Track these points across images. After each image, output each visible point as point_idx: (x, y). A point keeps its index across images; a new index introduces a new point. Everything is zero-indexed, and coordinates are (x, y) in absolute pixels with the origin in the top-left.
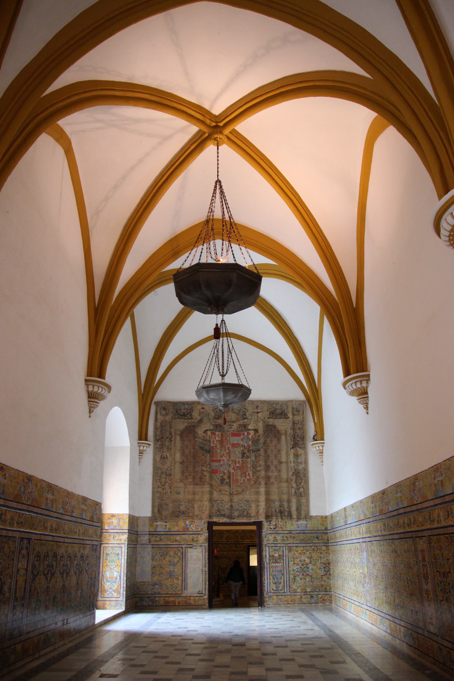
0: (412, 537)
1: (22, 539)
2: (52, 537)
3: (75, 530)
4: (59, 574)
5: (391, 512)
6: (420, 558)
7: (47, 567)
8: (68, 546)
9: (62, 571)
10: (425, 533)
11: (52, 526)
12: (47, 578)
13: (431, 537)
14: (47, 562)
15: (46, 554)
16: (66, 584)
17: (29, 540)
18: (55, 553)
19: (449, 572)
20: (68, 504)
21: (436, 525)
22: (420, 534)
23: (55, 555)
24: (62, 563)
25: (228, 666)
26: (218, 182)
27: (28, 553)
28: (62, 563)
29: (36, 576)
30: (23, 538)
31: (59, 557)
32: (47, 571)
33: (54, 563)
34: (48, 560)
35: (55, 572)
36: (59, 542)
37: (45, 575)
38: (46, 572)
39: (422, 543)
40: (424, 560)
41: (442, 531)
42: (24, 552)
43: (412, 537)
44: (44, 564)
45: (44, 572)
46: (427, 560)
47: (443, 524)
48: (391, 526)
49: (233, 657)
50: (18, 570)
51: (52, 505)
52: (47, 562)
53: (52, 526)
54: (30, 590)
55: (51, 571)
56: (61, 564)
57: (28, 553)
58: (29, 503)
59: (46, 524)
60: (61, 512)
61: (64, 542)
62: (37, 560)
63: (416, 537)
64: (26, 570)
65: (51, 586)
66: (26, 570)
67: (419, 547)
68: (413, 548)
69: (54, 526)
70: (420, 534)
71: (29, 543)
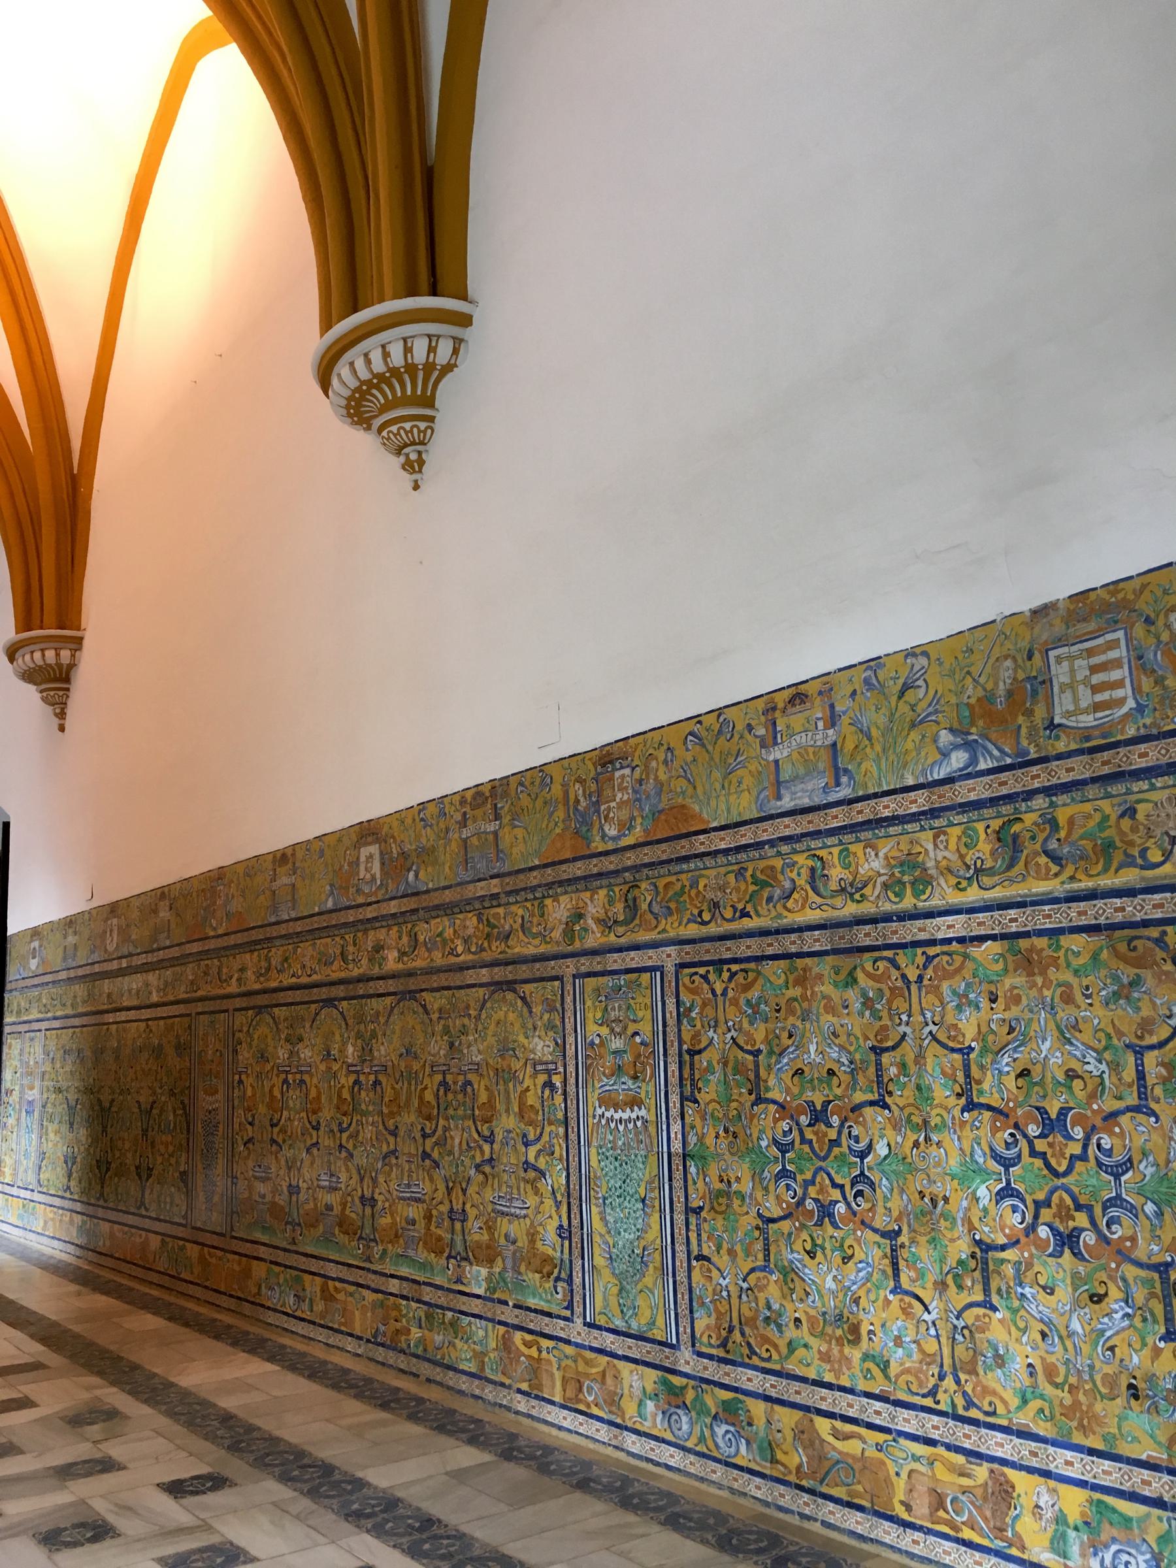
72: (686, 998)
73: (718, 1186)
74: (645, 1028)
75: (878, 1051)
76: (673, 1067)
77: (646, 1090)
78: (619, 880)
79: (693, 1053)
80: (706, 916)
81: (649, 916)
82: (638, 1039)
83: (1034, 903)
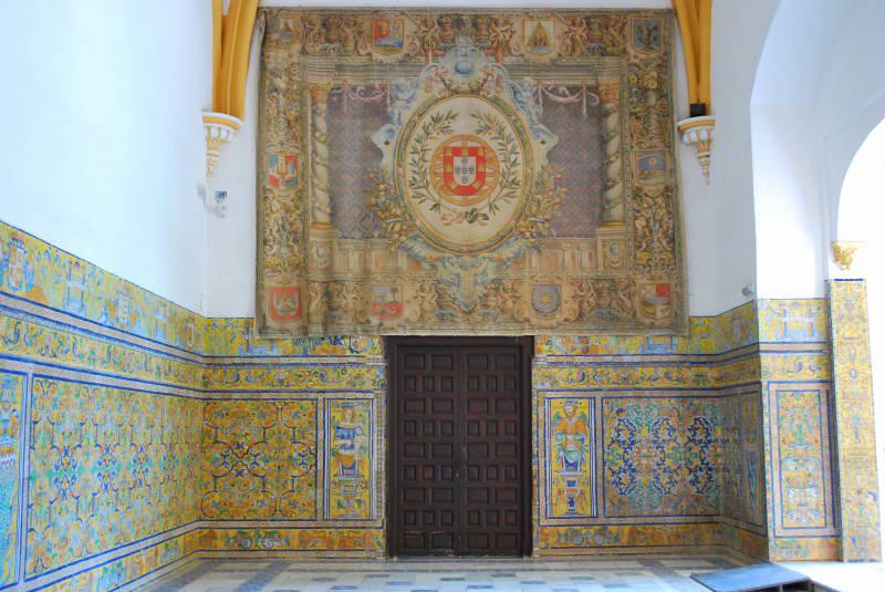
72: (35, 393)
73: (39, 491)
74: (18, 407)
75: (82, 424)
76: (28, 430)
77: (16, 443)
78: (16, 316)
79: (36, 423)
80: (44, 351)
81: (24, 343)
82: (15, 414)
83: (68, 369)
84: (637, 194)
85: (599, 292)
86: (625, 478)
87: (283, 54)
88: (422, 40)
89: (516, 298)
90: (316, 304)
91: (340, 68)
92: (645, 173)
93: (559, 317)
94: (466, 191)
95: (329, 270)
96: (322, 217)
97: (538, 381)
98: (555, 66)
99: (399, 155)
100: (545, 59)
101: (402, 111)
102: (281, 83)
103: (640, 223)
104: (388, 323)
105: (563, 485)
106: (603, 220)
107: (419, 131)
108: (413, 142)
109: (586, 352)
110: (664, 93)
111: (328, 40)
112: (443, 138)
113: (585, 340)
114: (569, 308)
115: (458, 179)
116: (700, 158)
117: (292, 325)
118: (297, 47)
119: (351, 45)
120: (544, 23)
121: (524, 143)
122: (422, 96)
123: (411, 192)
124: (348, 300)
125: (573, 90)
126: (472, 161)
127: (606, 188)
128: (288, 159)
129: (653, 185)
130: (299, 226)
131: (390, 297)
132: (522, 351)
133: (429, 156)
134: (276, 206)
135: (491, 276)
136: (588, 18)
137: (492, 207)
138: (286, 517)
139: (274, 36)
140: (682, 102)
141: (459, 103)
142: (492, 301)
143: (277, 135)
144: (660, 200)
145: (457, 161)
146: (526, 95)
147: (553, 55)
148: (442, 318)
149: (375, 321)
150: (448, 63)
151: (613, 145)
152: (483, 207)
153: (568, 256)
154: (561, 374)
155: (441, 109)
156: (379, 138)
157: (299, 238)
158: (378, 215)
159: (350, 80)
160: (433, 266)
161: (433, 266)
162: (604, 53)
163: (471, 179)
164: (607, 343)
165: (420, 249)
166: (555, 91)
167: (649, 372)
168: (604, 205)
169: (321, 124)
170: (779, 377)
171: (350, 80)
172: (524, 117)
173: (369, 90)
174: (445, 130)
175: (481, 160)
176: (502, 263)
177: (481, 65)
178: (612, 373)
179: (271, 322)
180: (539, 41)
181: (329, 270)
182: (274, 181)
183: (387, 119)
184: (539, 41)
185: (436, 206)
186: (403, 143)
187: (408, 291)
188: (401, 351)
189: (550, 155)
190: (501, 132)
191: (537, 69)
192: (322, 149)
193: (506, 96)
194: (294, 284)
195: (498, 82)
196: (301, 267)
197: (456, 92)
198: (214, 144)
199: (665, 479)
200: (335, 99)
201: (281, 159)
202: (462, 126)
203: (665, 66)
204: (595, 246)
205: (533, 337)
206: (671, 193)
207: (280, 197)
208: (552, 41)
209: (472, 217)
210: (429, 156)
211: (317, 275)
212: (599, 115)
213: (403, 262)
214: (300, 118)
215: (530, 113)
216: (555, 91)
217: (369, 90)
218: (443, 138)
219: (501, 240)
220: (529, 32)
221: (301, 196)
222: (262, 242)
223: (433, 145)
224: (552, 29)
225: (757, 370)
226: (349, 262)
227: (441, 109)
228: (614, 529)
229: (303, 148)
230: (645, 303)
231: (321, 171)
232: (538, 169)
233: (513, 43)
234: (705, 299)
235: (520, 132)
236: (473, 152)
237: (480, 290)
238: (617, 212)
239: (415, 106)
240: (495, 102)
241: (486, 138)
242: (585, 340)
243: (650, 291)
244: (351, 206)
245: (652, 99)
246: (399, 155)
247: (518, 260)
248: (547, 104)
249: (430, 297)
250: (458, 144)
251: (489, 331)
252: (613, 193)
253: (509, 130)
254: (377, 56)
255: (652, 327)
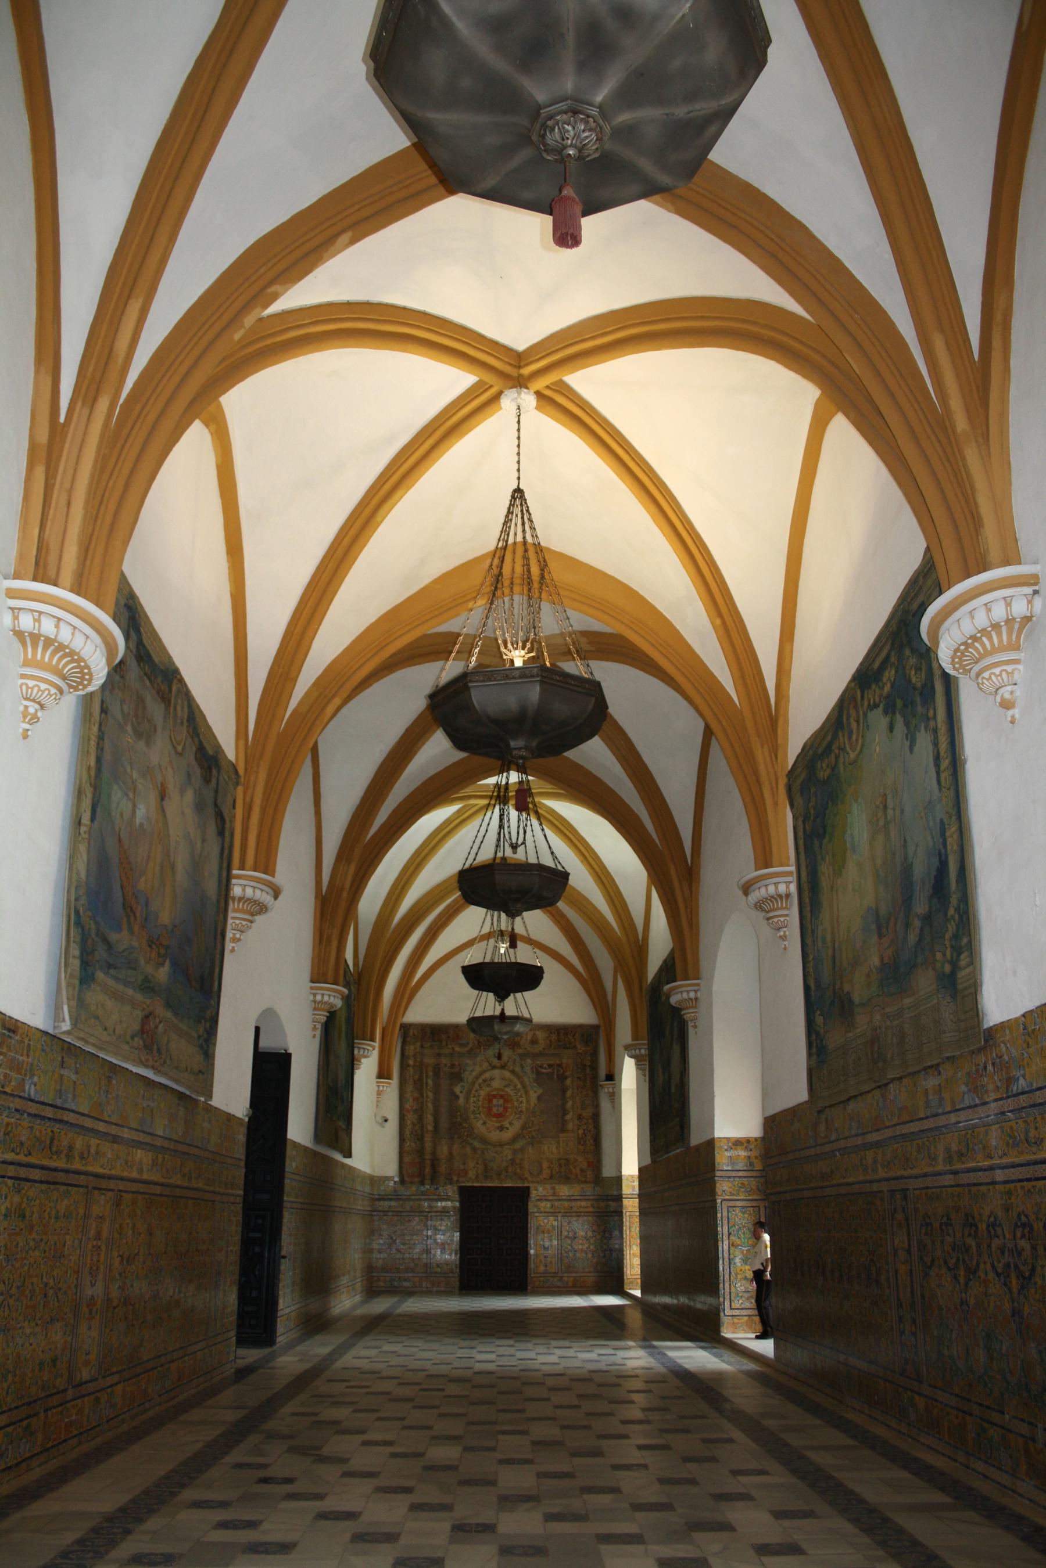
0: (87, 1187)
1: (892, 1192)
2: (952, 1176)
3: (1032, 1134)
4: (991, 1275)
5: (32, 1100)
6: (92, 1233)
7: (953, 1249)
8: (1009, 1193)
9: (1000, 1267)
10: (112, 1184)
11: (948, 1150)
12: (956, 1278)
13: (123, 1194)
14: (949, 1239)
15: (945, 1219)
16: (1027, 1310)
17: (904, 1191)
18: (967, 1215)
19: (137, 1254)
20: (990, 1067)
21: (134, 1174)
22: (104, 1184)
23: (970, 1222)
24: (996, 1243)
25: (501, 1462)
26: (518, 493)
27: (907, 1219)
28: (996, 1243)
29: (930, 1267)
30: (894, 1191)
31: (983, 1226)
32: (954, 1260)
33: (971, 1242)
34: (951, 1232)
35: (978, 1265)
36: (975, 1185)
37: (949, 1269)
38: (952, 1262)
39: (102, 1203)
40: (98, 1236)
41: (141, 1187)
42: (899, 1216)
43: (87, 1187)
44: (942, 1242)
45: (946, 1262)
46: (105, 1234)
47: (145, 1177)
48: (23, 1139)
49: (493, 1483)
50: (896, 1251)
51: (941, 1099)
52: (949, 1239)
53: (948, 1150)
54: (923, 1296)
55: (964, 1261)
56: (993, 1246)
57: (907, 1219)
58: (895, 1120)
59: (933, 1150)
60: (967, 1103)
61: (993, 1183)
62: (926, 1234)
63: (95, 1188)
64: (909, 1251)
65: (972, 1301)
66: (909, 1251)
67: (96, 1210)
68: (81, 1211)
69: (954, 1147)
70: (104, 1184)
71: (905, 1198)
84: (580, 1117)
85: (560, 1165)
86: (571, 1254)
87: (412, 1047)
88: (479, 1042)
89: (521, 1168)
90: (428, 1170)
91: (439, 1055)
92: (584, 1107)
93: (541, 1177)
94: (499, 1116)
95: (434, 1153)
96: (430, 1128)
97: (531, 1208)
98: (541, 1054)
99: (467, 1098)
100: (537, 1051)
101: (468, 1076)
102: (411, 1062)
103: (581, 1132)
104: (461, 1179)
105: (542, 1257)
106: (563, 1130)
107: (477, 1086)
108: (473, 1092)
109: (554, 1194)
110: (594, 1067)
111: (433, 1041)
112: (488, 1089)
113: (553, 1188)
114: (546, 1173)
115: (495, 1110)
116: (768, 919)
117: (416, 1180)
118: (419, 1044)
119: (444, 1043)
120: (537, 1033)
121: (527, 1093)
122: (478, 1069)
123: (472, 1116)
124: (443, 1168)
125: (550, 1066)
126: (501, 1101)
127: (565, 1114)
128: (414, 1099)
129: (588, 1112)
130: (419, 1132)
131: (462, 1167)
132: (523, 1194)
133: (481, 1099)
134: (409, 1122)
135: (510, 1157)
136: (558, 1030)
137: (511, 1124)
138: (412, 1271)
139: (409, 1039)
140: (602, 1073)
141: (496, 1073)
142: (510, 1169)
143: (409, 1088)
144: (590, 1121)
145: (495, 1101)
146: (528, 1069)
147: (541, 1049)
148: (486, 1178)
149: (455, 1178)
150: (491, 1052)
151: (569, 1093)
152: (506, 1123)
153: (546, 1147)
154: (545, 1205)
155: (487, 1075)
156: (457, 1090)
157: (421, 1139)
158: (457, 1126)
159: (444, 1061)
160: (483, 1153)
161: (483, 1153)
162: (566, 1048)
163: (501, 1109)
164: (564, 1190)
165: (477, 1144)
166: (541, 1067)
167: (584, 1204)
168: (564, 1123)
169: (430, 1082)
170: (630, 1209)
171: (444, 1061)
172: (526, 1080)
173: (453, 1066)
174: (489, 1086)
175: (506, 1101)
176: (515, 1152)
177: (507, 1053)
178: (566, 1204)
179: (406, 1179)
180: (534, 1042)
181: (434, 1153)
182: (408, 1111)
183: (462, 1080)
184: (534, 1042)
185: (484, 1123)
186: (469, 1092)
187: (471, 1164)
188: (467, 1195)
189: (539, 1098)
190: (516, 1086)
191: (534, 1056)
192: (430, 1095)
193: (518, 1069)
194: (417, 1160)
195: (515, 1061)
196: (421, 1152)
197: (494, 1067)
198: (379, 1093)
199: (590, 1256)
200: (437, 1070)
201: (411, 1100)
202: (496, 1084)
203: (595, 1053)
204: (558, 1143)
205: (528, 1188)
206: (596, 1117)
207: (411, 1118)
208: (541, 1041)
209: (501, 1128)
210: (481, 1099)
211: (428, 1156)
212: (562, 1078)
213: (468, 1150)
214: (420, 1079)
215: (529, 1077)
216: (541, 1067)
217: (453, 1066)
218: (488, 1089)
219: (514, 1140)
220: (529, 1038)
221: (421, 1118)
222: (402, 1140)
223: (482, 1093)
224: (540, 1035)
225: (621, 1206)
226: (443, 1150)
227: (487, 1075)
228: (566, 1279)
229: (422, 1095)
230: (582, 1171)
231: (430, 1105)
232: (532, 1104)
233: (522, 1043)
234: (607, 1172)
235: (524, 1086)
236: (502, 1097)
237: (504, 1164)
238: (570, 1126)
239: (474, 1074)
240: (513, 1072)
241: (508, 1090)
242: (553, 1188)
243: (584, 1165)
244: (444, 1124)
245: (588, 1071)
246: (467, 1098)
247: (522, 1149)
248: (538, 1073)
249: (481, 1167)
250: (495, 1093)
251: (509, 1184)
252: (568, 1117)
253: (519, 1086)
254: (457, 1049)
255: (585, 1182)
